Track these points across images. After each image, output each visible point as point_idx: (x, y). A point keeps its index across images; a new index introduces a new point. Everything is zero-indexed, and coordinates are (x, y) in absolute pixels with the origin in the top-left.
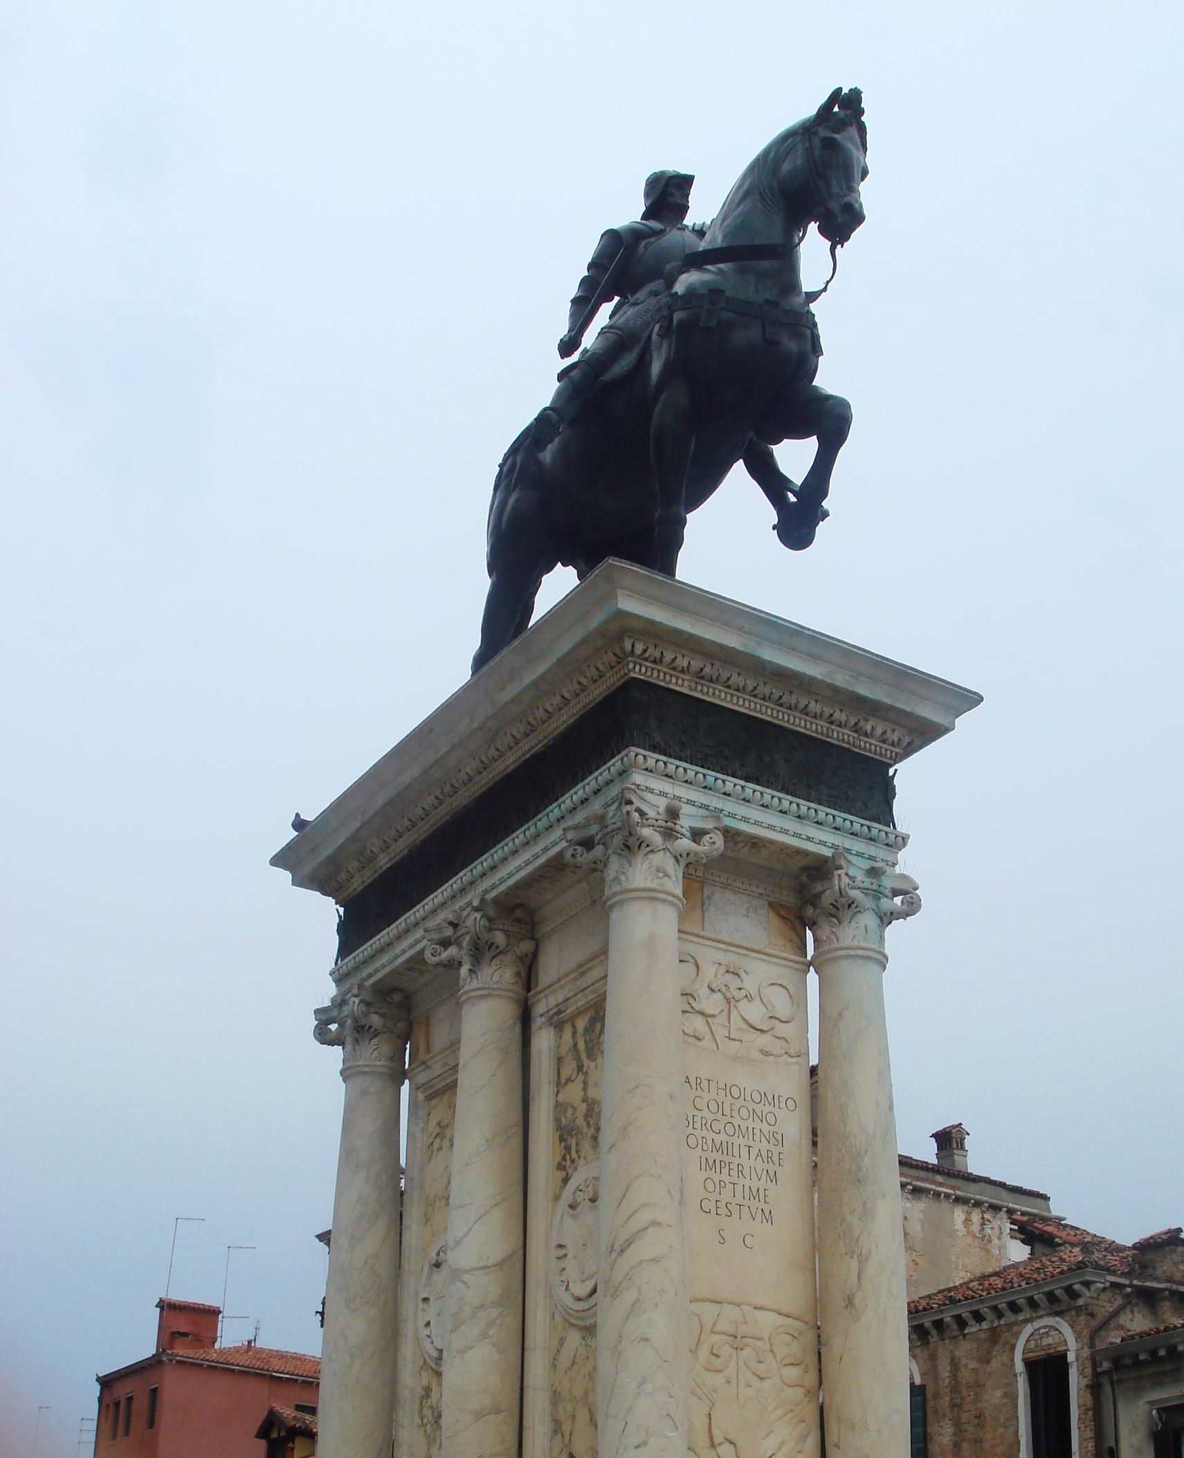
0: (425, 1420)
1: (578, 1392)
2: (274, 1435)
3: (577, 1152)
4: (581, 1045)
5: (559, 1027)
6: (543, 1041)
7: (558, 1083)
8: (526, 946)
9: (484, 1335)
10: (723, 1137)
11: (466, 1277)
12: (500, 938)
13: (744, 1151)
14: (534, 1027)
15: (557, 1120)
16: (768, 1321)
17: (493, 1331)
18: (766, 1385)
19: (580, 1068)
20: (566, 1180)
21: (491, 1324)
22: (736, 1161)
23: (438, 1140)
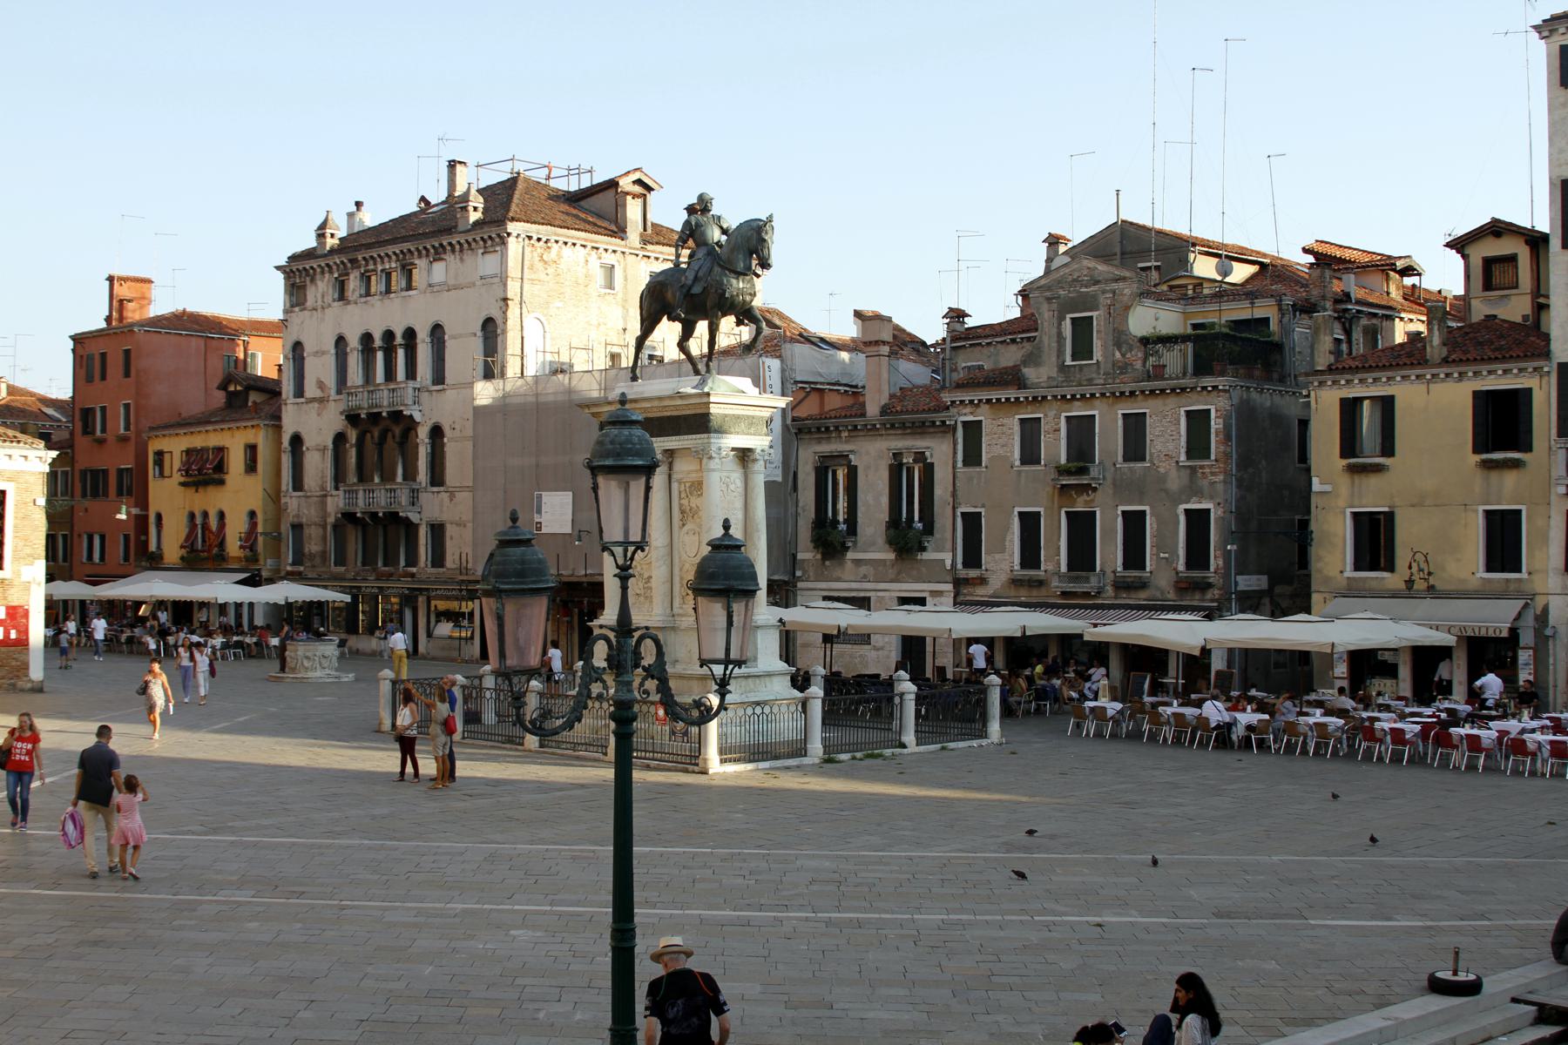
2: (232, 388)
5: (680, 483)
6: (675, 486)
20: (684, 525)
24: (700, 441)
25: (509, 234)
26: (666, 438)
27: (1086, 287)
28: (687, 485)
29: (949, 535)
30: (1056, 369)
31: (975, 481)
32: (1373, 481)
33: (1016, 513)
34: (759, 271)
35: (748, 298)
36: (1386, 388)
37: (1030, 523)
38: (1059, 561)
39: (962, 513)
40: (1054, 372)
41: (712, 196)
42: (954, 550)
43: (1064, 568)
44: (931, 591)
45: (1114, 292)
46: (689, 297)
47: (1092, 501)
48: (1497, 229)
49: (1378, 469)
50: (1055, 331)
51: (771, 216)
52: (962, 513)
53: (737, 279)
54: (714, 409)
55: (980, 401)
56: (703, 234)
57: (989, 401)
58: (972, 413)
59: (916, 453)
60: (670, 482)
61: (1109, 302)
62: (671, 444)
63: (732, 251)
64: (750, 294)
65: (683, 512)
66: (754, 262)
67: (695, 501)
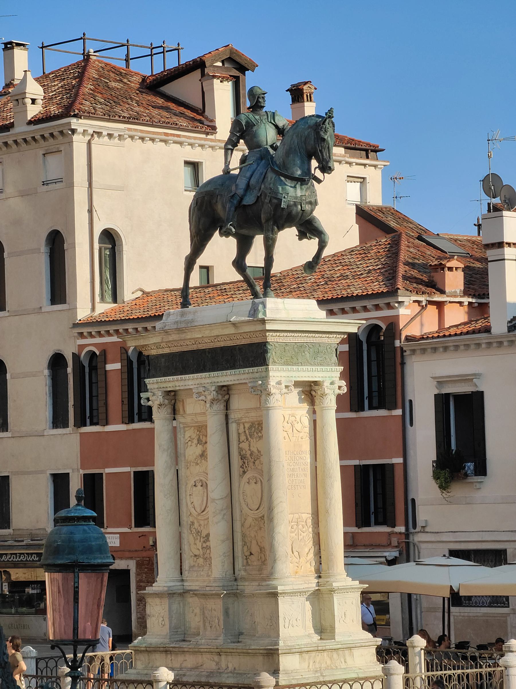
0: (192, 532)
1: (253, 536)
3: (248, 465)
4: (247, 432)
5: (238, 424)
6: (233, 427)
7: (239, 441)
8: (227, 397)
9: (223, 518)
10: (293, 467)
11: (217, 502)
12: (220, 397)
13: (298, 469)
14: (230, 421)
16: (305, 516)
17: (225, 517)
18: (305, 534)
19: (247, 439)
20: (244, 472)
21: (224, 514)
22: (296, 473)
23: (190, 442)
25: (74, 131)
26: (220, 373)
28: (247, 426)
34: (318, 174)
35: (307, 208)
41: (264, 90)
46: (240, 207)
51: (331, 111)
53: (295, 187)
54: (271, 338)
56: (255, 135)
60: (227, 424)
62: (226, 379)
63: (288, 153)
64: (310, 203)
65: (243, 457)
66: (314, 163)
67: (255, 445)
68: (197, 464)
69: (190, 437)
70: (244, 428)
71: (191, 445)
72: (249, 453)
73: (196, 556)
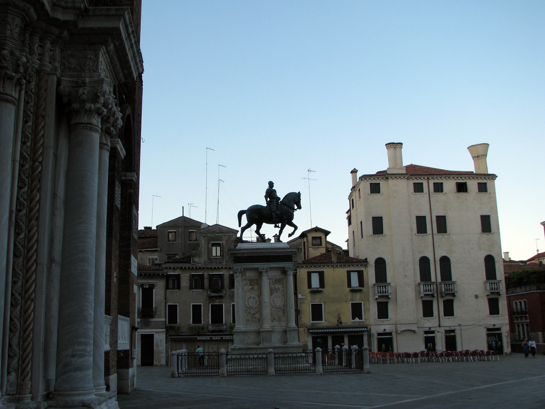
4: (274, 282)
15: (270, 289)
20: (272, 294)
23: (246, 285)
24: (287, 265)
27: (218, 234)
29: (163, 312)
30: (207, 259)
31: (175, 294)
32: (318, 296)
33: (191, 305)
36: (322, 269)
37: (197, 309)
38: (209, 320)
39: (168, 305)
40: (207, 260)
42: (166, 318)
43: (210, 323)
44: (156, 332)
45: (229, 236)
47: (222, 301)
48: (317, 230)
49: (320, 292)
50: (207, 246)
52: (168, 305)
55: (178, 268)
57: (181, 268)
58: (173, 272)
59: (149, 285)
61: (227, 239)
68: (249, 291)
69: (246, 283)
70: (272, 281)
71: (247, 286)
72: (274, 289)
73: (248, 320)
